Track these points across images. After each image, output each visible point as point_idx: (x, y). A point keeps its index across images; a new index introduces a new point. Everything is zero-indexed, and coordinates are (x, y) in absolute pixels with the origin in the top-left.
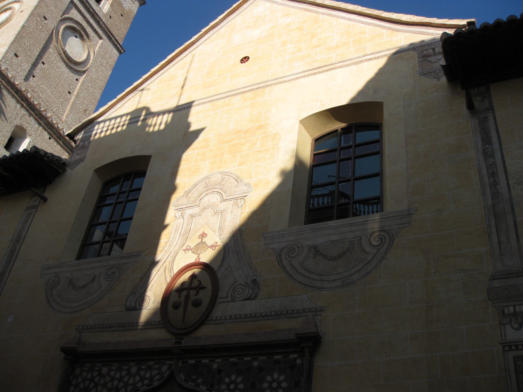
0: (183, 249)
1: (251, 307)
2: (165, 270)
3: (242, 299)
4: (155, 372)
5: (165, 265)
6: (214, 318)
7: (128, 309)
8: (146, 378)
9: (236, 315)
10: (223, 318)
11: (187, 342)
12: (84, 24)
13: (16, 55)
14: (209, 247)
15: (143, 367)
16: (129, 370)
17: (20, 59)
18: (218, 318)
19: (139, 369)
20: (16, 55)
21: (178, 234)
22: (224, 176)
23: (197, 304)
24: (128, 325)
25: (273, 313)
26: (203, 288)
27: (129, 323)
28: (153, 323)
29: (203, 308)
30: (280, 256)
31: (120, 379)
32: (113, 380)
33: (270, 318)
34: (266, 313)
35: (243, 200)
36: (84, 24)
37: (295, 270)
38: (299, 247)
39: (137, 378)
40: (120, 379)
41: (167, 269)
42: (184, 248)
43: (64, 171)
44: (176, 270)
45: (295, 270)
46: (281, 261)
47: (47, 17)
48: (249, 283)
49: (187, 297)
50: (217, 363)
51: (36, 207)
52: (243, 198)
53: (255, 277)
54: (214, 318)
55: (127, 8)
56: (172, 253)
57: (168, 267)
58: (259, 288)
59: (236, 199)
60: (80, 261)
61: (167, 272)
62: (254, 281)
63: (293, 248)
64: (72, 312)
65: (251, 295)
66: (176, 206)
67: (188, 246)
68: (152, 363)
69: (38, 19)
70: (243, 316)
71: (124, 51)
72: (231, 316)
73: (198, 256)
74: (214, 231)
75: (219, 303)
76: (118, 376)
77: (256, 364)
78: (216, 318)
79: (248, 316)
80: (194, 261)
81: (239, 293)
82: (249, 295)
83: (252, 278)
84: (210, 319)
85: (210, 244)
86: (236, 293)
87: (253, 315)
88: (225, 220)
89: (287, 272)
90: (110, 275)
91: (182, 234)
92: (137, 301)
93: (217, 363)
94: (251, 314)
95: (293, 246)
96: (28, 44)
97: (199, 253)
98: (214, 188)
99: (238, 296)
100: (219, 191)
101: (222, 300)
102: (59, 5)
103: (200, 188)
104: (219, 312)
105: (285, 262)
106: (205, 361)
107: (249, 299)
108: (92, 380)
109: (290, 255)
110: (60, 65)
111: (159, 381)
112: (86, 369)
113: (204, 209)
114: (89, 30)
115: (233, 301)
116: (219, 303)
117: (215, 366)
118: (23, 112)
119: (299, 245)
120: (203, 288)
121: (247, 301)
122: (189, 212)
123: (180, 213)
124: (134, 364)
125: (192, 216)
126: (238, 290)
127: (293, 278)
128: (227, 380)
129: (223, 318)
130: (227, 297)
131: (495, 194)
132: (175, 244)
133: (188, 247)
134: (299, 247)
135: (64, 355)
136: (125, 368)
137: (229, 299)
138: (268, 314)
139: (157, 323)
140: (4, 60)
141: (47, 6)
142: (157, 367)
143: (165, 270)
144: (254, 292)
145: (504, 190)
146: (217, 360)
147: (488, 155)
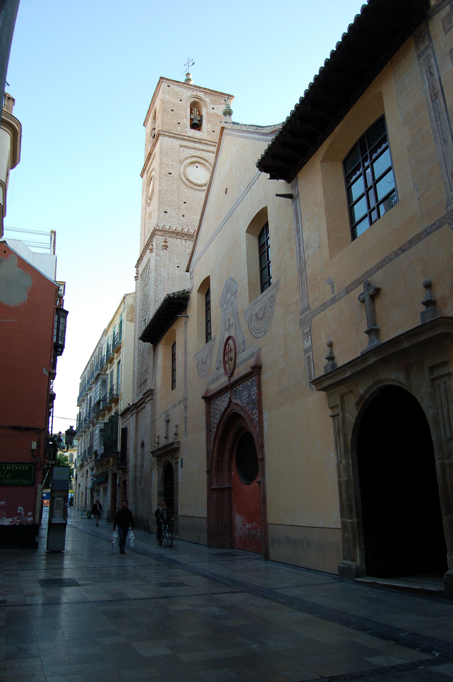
13: (166, 212)
17: (168, 212)
19: (224, 398)
20: (166, 212)
36: (199, 153)
47: (170, 172)
51: (186, 322)
59: (234, 294)
69: (166, 178)
102: (174, 157)
103: (225, 290)
106: (238, 387)
107: (243, 351)
114: (202, 154)
131: (300, 258)
140: (160, 221)
145: (303, 256)
147: (298, 231)
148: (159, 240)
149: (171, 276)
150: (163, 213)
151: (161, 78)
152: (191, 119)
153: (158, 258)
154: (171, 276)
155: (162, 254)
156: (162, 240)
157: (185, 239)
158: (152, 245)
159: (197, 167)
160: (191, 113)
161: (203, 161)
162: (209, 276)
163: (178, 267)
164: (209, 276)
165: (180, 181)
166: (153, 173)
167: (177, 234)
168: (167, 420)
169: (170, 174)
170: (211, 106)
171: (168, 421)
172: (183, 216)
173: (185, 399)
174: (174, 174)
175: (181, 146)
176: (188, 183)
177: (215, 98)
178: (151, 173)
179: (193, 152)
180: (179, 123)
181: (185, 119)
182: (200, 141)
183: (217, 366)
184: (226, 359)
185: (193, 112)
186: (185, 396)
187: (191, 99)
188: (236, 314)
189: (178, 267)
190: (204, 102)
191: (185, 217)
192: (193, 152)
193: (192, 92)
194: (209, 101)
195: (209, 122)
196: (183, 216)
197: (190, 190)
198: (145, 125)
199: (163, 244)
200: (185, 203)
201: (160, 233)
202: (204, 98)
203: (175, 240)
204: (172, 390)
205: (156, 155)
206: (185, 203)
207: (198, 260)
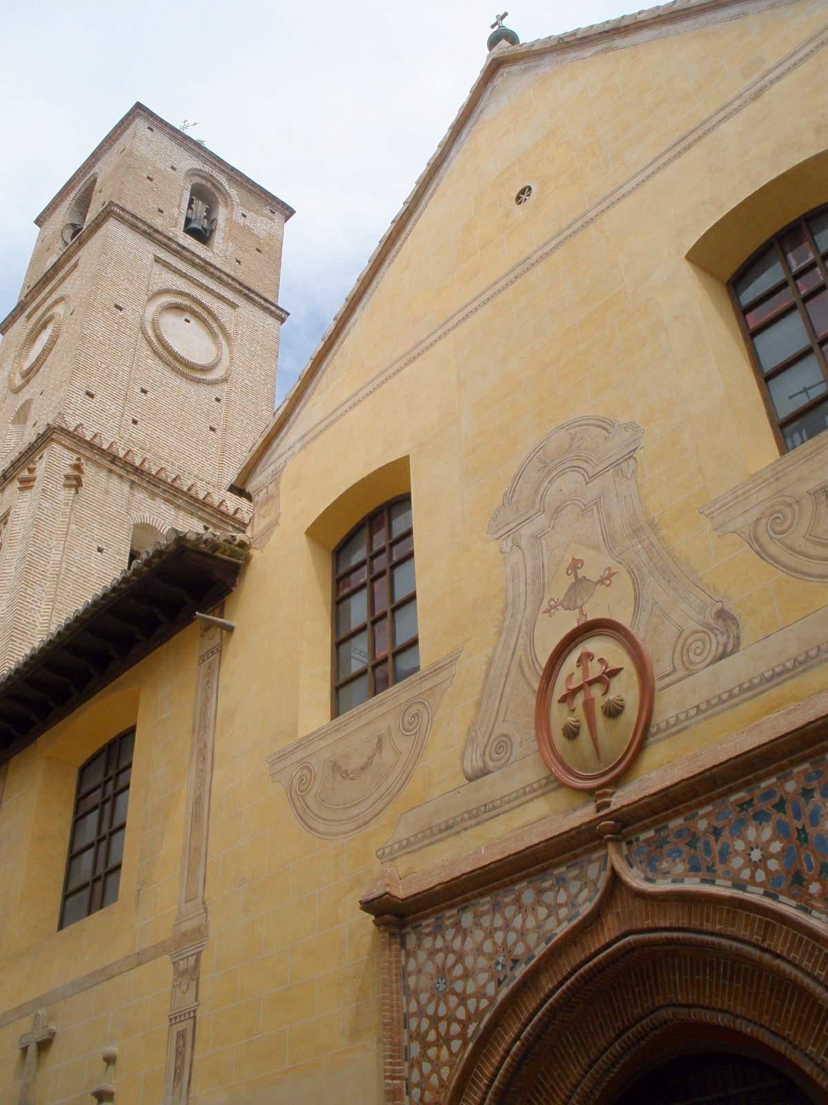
0: (541, 611)
1: (734, 671)
2: (521, 668)
3: (708, 661)
4: (574, 886)
5: (516, 658)
6: (663, 725)
7: (470, 779)
8: (560, 906)
9: (708, 702)
10: (682, 717)
11: (622, 798)
12: (196, 292)
14: (596, 584)
15: (547, 884)
16: (517, 900)
17: (98, 397)
18: (672, 721)
21: (522, 585)
22: (572, 431)
23: (614, 712)
24: (483, 809)
25: (789, 665)
26: (614, 673)
27: (485, 805)
28: (536, 786)
29: (631, 713)
30: (757, 541)
31: (507, 927)
32: (490, 934)
33: (784, 677)
34: (773, 670)
35: (631, 461)
36: (196, 292)
37: (800, 553)
38: (790, 505)
39: (542, 912)
40: (507, 927)
41: (525, 665)
42: (545, 605)
43: (248, 559)
44: (543, 660)
45: (800, 553)
46: (764, 550)
47: (121, 305)
48: (711, 621)
49: (588, 705)
50: (703, 817)
52: (630, 456)
53: (719, 606)
54: (663, 725)
55: (263, 235)
56: (524, 628)
57: (524, 659)
58: (738, 627)
59: (617, 464)
60: (341, 718)
61: (526, 670)
62: (722, 614)
63: (779, 512)
64: (358, 828)
65: (725, 646)
66: (496, 532)
67: (552, 599)
68: (563, 869)
70: (725, 697)
71: (288, 314)
72: (698, 707)
73: (581, 612)
74: (595, 547)
75: (663, 689)
76: (499, 922)
77: (791, 786)
78: (667, 722)
79: (736, 691)
80: (576, 625)
81: (698, 651)
82: (721, 648)
83: (714, 611)
84: (653, 730)
85: (595, 578)
86: (691, 654)
87: (746, 686)
88: (609, 518)
89: (784, 566)
90: (411, 724)
91: (528, 581)
92: (484, 754)
93: (703, 817)
94: (740, 686)
95: (777, 508)
96: (103, 366)
97: (579, 603)
98: (561, 463)
99: (698, 659)
100: (575, 463)
101: (667, 681)
102: (136, 274)
104: (667, 707)
105: (773, 549)
107: (723, 656)
108: (448, 949)
109: (778, 529)
110: (175, 383)
111: (590, 901)
112: (427, 930)
113: (558, 510)
115: (691, 673)
116: (663, 689)
117: (702, 825)
118: (140, 495)
119: (790, 500)
120: (614, 673)
121: (722, 661)
122: (527, 531)
123: (509, 540)
124: (524, 884)
125: (536, 538)
126: (694, 646)
127: (802, 573)
128: (740, 845)
129: (682, 717)
130: (675, 670)
132: (522, 607)
133: (552, 603)
134: (790, 505)
135: (373, 917)
136: (508, 900)
137: (681, 673)
138: (778, 670)
139: (544, 782)
141: (114, 284)
142: (574, 873)
143: (521, 668)
144: (728, 638)
146: (701, 812)
148: (57, 459)
149: (75, 570)
150: (82, 393)
151: (139, 106)
152: (188, 221)
153: (47, 505)
154: (75, 570)
155: (61, 498)
156: (69, 462)
157: (133, 483)
158: (31, 471)
159: (187, 321)
160: (190, 207)
161: (205, 315)
162: (407, 458)
163: (100, 550)
164: (407, 458)
165: (140, 335)
166: (59, 310)
167: (114, 459)
168: (40, 1035)
169: (121, 309)
170: (239, 210)
171: (44, 1045)
172: (135, 422)
173: (200, 933)
174: (128, 312)
175: (157, 260)
176: (160, 349)
177: (251, 199)
178: (52, 306)
179: (182, 285)
180: (161, 211)
181: (176, 209)
182: (205, 267)
183: (474, 762)
184: (559, 716)
185: (193, 206)
186: (187, 926)
187: (197, 178)
188: (636, 532)
189: (100, 550)
190: (227, 196)
191: (138, 427)
192: (182, 285)
193: (201, 163)
194: (236, 197)
195: (230, 237)
196: (135, 422)
197: (161, 367)
198: (39, 222)
199: (69, 471)
200: (144, 391)
201: (67, 441)
202: (227, 187)
203: (103, 474)
204: (61, 927)
205: (81, 265)
206: (144, 391)
207: (307, 440)
